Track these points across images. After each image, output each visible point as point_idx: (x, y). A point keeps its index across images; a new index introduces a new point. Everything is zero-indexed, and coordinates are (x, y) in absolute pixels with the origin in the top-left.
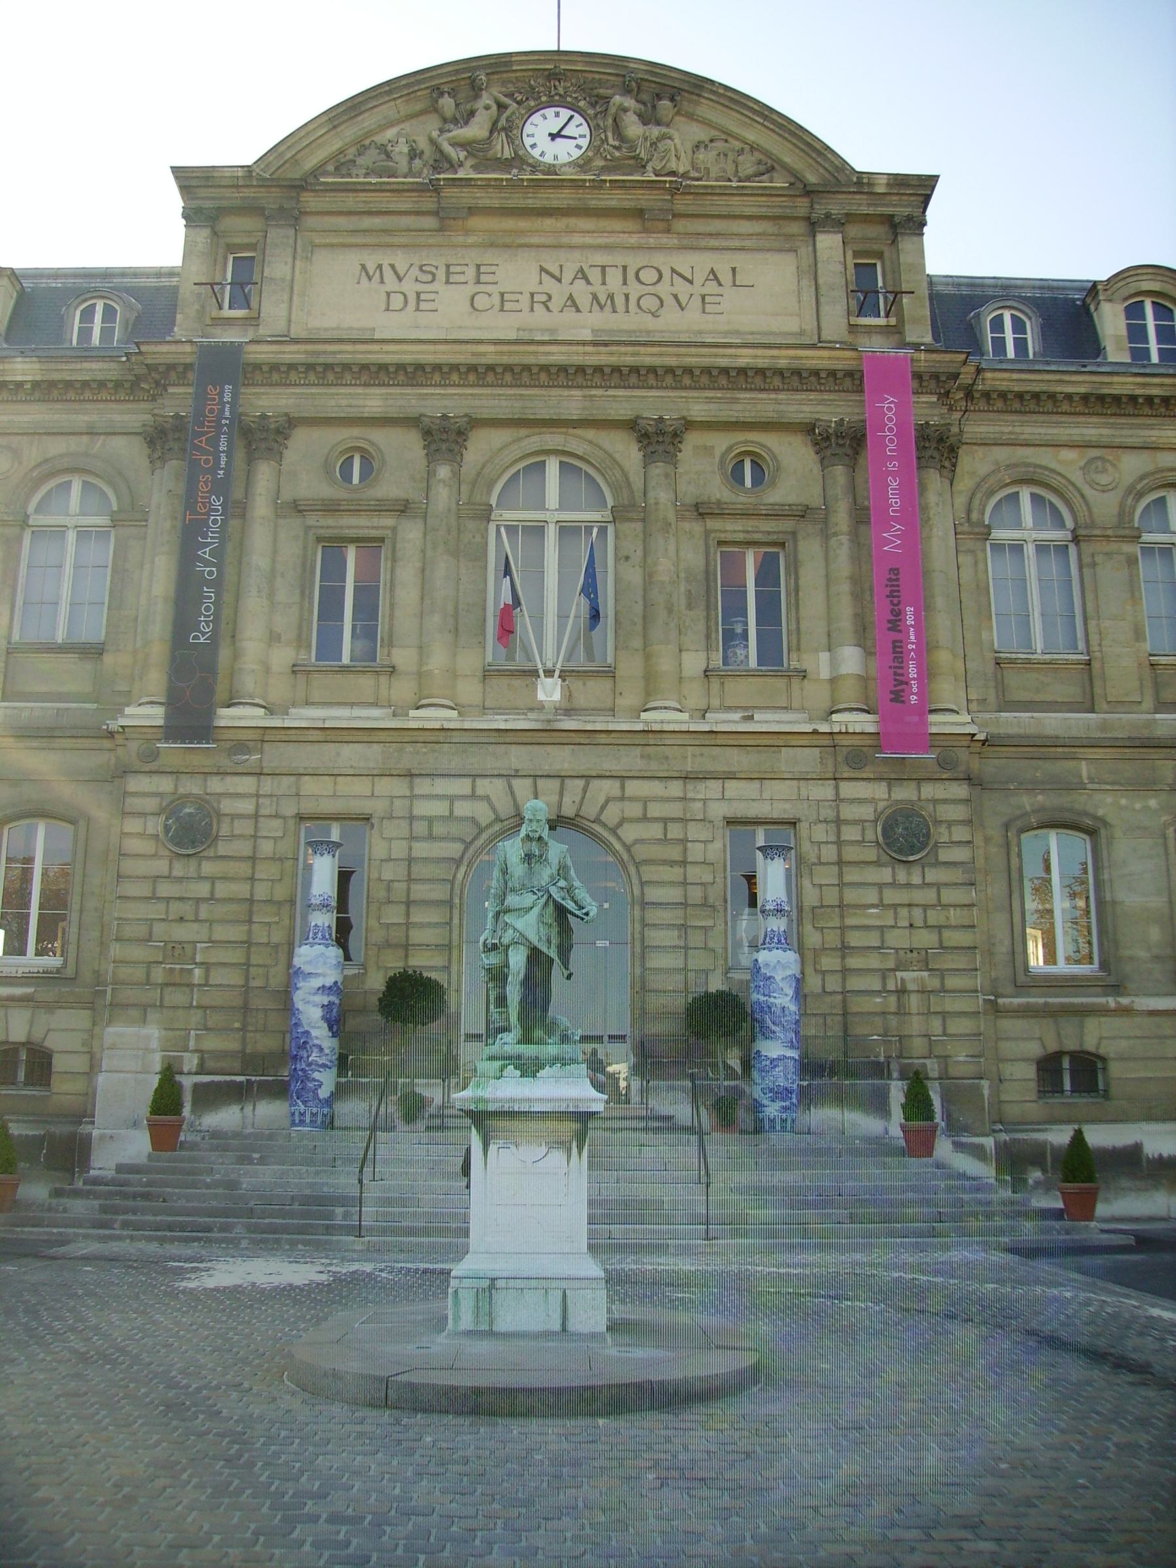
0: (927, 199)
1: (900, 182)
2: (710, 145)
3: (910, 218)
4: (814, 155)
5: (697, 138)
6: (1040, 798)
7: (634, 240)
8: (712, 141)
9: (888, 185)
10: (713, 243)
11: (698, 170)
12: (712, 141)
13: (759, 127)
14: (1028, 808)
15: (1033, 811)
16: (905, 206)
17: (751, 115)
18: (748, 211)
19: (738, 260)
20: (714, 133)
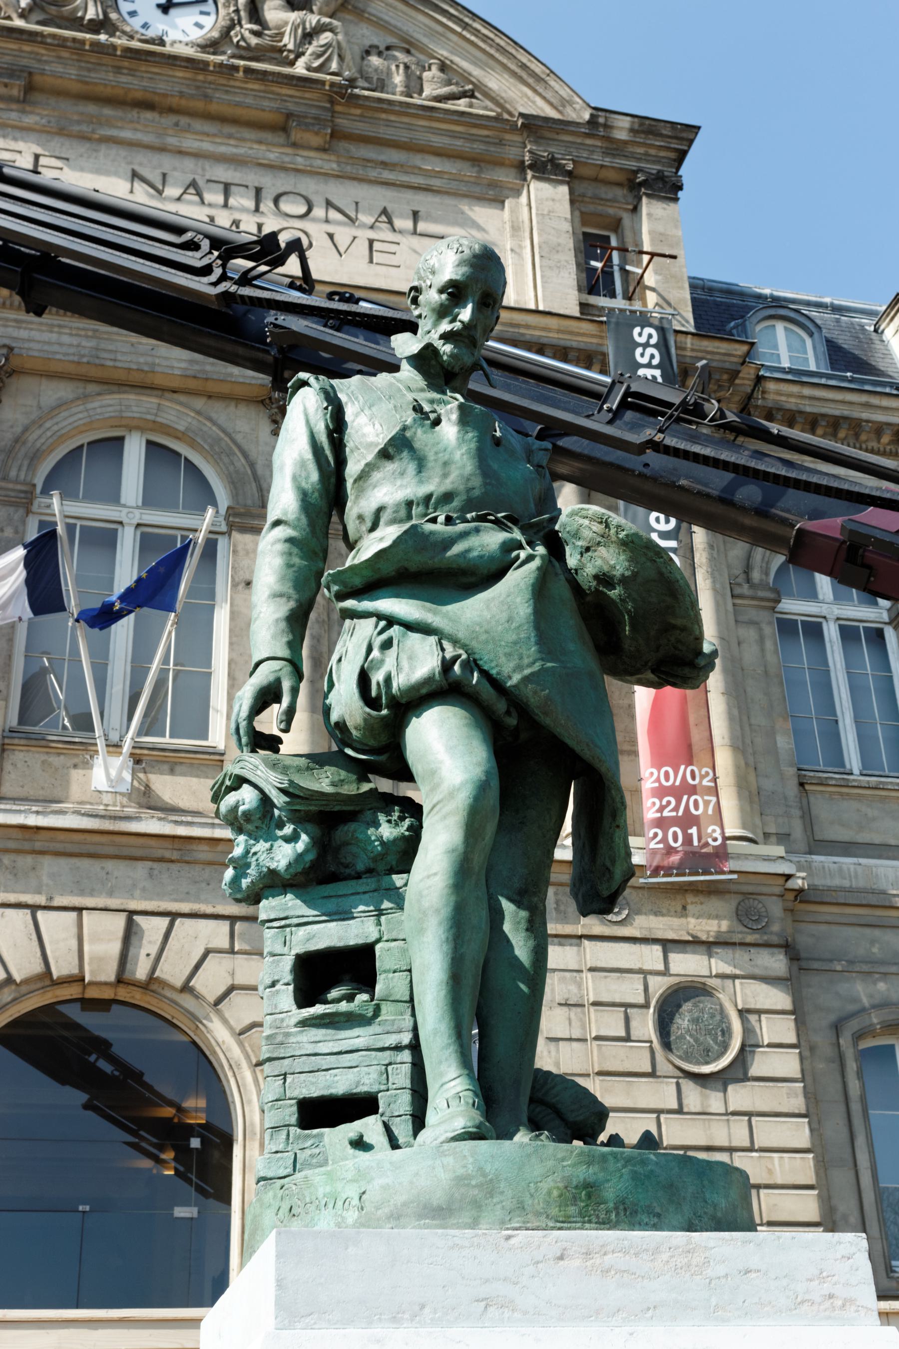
0: (681, 156)
1: (647, 127)
2: (386, 53)
3: (660, 177)
4: (531, 81)
5: (367, 43)
6: (882, 986)
7: (273, 155)
8: (388, 48)
9: (632, 130)
10: (387, 175)
11: (368, 79)
12: (388, 48)
13: (454, 38)
14: (866, 1002)
15: (874, 1007)
16: (654, 162)
17: (444, 20)
18: (438, 141)
19: (422, 201)
20: (391, 40)
